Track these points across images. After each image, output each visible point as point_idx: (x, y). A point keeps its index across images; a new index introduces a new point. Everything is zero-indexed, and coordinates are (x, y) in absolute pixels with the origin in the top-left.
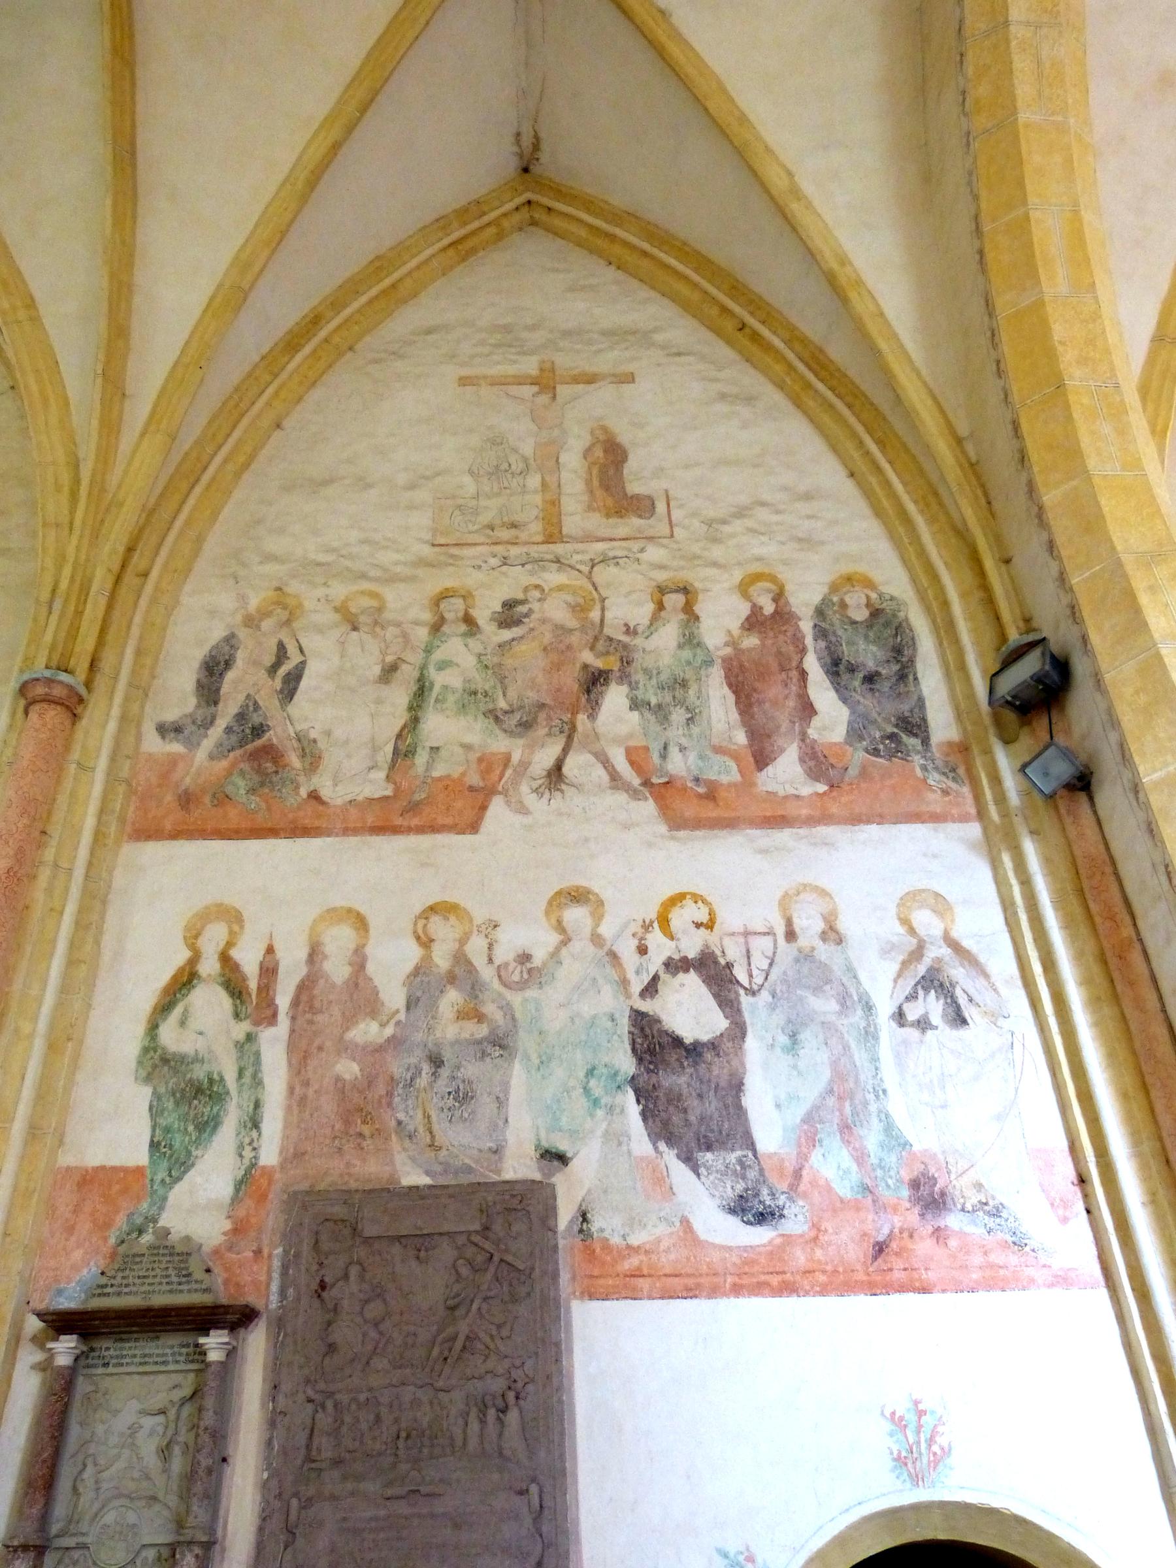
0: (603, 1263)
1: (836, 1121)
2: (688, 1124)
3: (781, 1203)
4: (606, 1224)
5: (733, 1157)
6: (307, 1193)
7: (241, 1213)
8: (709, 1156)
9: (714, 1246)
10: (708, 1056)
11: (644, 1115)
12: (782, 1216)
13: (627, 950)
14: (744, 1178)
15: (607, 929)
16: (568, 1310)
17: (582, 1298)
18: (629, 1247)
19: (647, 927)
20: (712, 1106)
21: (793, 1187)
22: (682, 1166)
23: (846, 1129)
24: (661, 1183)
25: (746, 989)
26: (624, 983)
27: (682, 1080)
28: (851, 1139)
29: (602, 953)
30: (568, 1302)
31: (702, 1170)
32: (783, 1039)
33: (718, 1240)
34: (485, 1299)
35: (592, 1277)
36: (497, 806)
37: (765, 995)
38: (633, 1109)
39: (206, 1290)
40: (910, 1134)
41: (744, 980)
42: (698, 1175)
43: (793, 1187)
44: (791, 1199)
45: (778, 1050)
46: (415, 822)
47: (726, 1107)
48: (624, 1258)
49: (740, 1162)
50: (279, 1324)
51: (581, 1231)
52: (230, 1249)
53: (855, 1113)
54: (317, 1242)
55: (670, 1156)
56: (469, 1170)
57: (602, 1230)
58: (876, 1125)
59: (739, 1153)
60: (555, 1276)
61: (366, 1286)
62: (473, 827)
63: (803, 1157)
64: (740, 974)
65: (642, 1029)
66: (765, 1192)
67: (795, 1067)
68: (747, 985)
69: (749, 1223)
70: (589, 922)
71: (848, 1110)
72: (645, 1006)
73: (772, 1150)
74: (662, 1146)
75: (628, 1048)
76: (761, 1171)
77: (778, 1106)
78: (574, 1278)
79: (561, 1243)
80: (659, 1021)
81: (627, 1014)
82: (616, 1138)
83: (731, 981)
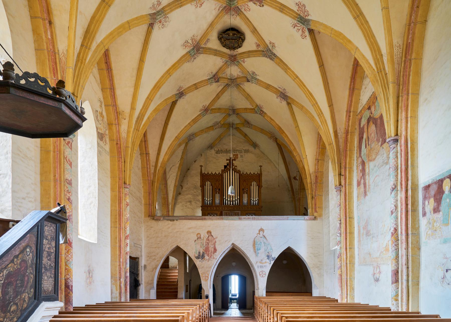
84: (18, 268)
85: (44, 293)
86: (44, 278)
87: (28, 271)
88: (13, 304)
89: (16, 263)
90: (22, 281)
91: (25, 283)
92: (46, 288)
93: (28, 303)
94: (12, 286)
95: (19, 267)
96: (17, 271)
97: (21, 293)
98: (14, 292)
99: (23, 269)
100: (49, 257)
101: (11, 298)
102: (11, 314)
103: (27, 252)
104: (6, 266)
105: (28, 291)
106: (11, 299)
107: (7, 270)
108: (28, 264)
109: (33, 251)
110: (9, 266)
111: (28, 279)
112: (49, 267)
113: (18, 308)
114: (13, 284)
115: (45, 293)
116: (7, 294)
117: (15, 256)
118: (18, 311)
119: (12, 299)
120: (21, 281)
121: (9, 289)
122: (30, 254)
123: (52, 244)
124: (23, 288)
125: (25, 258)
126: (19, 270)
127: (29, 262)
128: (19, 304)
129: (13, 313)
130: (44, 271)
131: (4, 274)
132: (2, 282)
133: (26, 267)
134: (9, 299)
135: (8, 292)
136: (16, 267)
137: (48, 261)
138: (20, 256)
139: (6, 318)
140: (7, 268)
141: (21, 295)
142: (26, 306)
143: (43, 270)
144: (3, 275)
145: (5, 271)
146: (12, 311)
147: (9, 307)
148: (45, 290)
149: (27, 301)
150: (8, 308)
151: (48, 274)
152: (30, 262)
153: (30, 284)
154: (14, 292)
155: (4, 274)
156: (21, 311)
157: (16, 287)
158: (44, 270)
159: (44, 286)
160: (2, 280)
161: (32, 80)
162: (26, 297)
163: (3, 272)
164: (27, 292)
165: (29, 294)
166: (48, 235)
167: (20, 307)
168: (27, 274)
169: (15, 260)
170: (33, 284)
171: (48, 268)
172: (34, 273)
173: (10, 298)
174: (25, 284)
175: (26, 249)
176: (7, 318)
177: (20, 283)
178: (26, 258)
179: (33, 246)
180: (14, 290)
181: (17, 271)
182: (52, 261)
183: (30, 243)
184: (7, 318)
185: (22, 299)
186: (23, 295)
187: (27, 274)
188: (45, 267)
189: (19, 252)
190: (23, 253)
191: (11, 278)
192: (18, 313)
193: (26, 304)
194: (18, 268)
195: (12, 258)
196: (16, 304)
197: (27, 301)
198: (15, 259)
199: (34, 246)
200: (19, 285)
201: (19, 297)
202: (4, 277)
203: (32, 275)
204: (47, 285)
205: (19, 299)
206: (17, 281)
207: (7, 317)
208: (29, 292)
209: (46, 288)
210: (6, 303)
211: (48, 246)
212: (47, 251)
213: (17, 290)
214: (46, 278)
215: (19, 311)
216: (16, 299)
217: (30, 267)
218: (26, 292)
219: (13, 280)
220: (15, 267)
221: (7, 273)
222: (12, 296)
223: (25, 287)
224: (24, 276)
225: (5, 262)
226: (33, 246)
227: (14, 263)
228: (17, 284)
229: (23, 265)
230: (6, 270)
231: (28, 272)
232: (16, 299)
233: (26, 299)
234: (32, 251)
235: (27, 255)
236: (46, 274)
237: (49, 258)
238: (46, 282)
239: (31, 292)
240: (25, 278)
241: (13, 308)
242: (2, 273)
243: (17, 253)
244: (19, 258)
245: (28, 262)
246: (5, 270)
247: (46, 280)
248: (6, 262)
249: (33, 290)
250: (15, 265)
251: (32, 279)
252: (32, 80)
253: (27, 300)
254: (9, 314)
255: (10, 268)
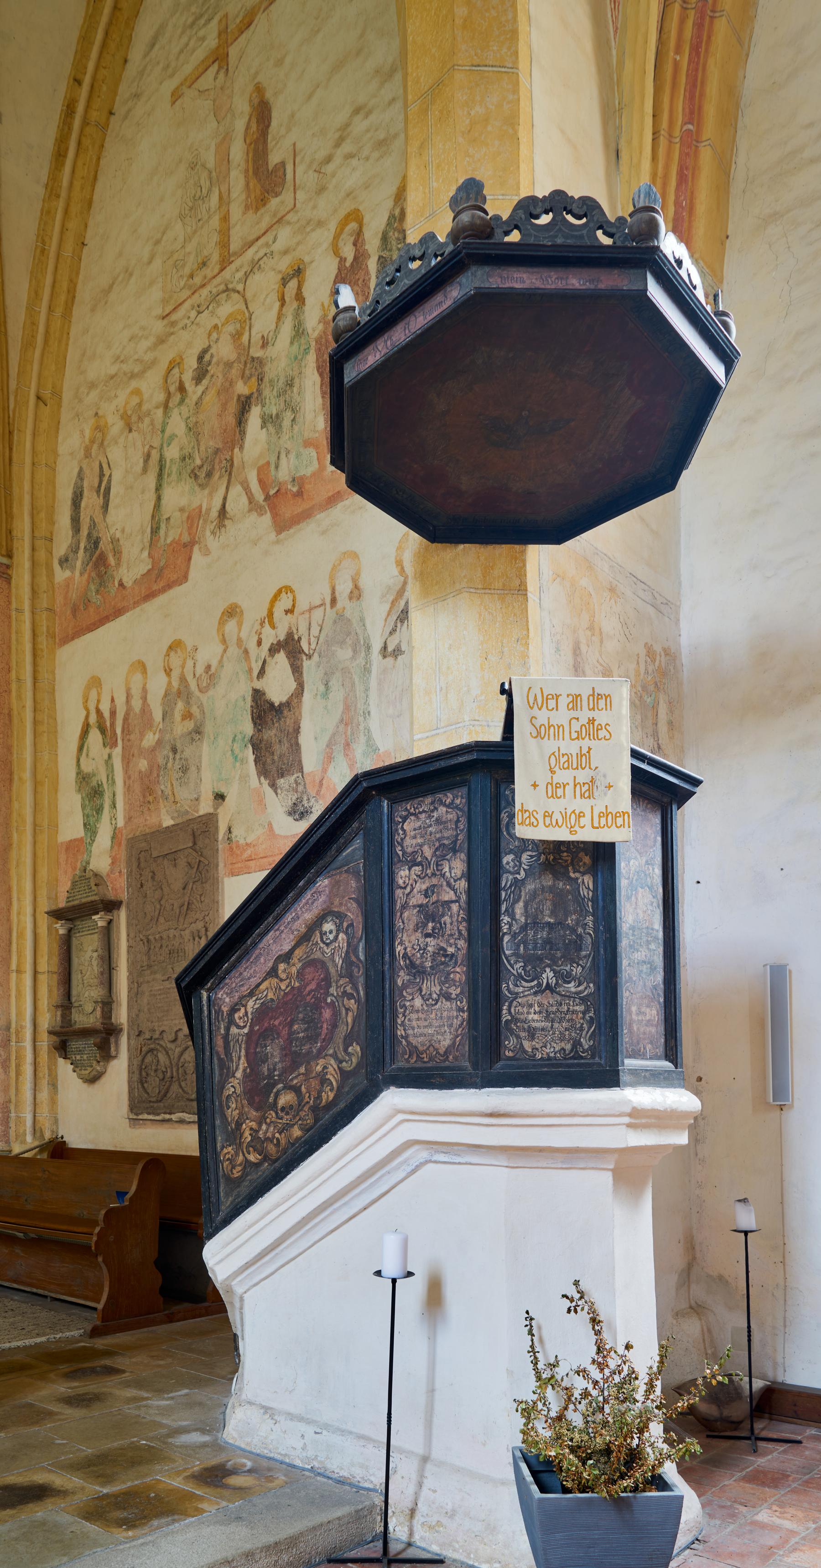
0: (237, 855)
1: (343, 741)
2: (273, 761)
3: (311, 804)
4: (238, 833)
5: (292, 779)
6: (132, 838)
7: (114, 854)
8: (282, 780)
9: (281, 836)
10: (285, 712)
11: (256, 761)
12: (311, 812)
13: (252, 645)
14: (297, 792)
15: (243, 635)
16: (223, 883)
17: (228, 876)
18: (247, 844)
19: (262, 624)
20: (286, 746)
21: (318, 793)
22: (270, 789)
23: (347, 745)
24: (261, 802)
25: (306, 655)
26: (250, 670)
27: (272, 733)
28: (349, 753)
29: (241, 651)
30: (223, 879)
31: (279, 791)
32: (322, 688)
33: (283, 834)
34: (194, 882)
35: (232, 864)
36: (196, 555)
37: (316, 657)
38: (251, 758)
39: (96, 895)
40: (379, 744)
41: (306, 651)
42: (277, 794)
43: (318, 793)
44: (317, 801)
45: (319, 697)
46: (162, 584)
47: (291, 745)
48: (245, 850)
49: (296, 782)
50: (128, 907)
51: (228, 839)
52: (111, 872)
53: (353, 734)
54: (139, 864)
55: (265, 783)
56: (187, 812)
57: (236, 836)
58: (362, 739)
59: (295, 775)
60: (217, 866)
61: (155, 883)
62: (185, 578)
63: (325, 770)
64: (304, 645)
65: (257, 703)
66: (305, 798)
67: (326, 707)
68: (307, 652)
69: (296, 820)
70: (236, 630)
71: (349, 733)
72: (258, 685)
73: (311, 770)
74: (262, 778)
75: (250, 717)
76: (305, 784)
77: (316, 738)
78: (225, 866)
79: (220, 847)
80: (264, 694)
81: (250, 692)
82: (244, 778)
83: (300, 653)
84: (293, 988)
85: (410, 1055)
86: (408, 1004)
87: (333, 990)
88: (284, 1088)
89: (283, 976)
90: (312, 1024)
91: (322, 1027)
92: (420, 1039)
93: (338, 1088)
94: (278, 1038)
95: (297, 984)
96: (290, 997)
97: (309, 1058)
98: (286, 1055)
99: (313, 986)
100: (430, 925)
101: (275, 1070)
102: (281, 1114)
103: (322, 934)
104: (252, 990)
105: (335, 1052)
106: (276, 1073)
107: (257, 999)
108: (332, 971)
109: (351, 925)
110: (263, 987)
111: (336, 1014)
112: (433, 960)
113: (302, 1100)
114: (278, 1034)
115: (418, 1056)
116: (264, 1062)
117: (280, 956)
118: (301, 1110)
119: (279, 1076)
120: (308, 1023)
121: (266, 1046)
122: (336, 938)
123: (447, 869)
124: (317, 1043)
125: (318, 955)
126: (295, 992)
127: (334, 961)
128: (303, 1089)
129: (287, 1114)
130: (409, 981)
131: (250, 1010)
132: (246, 1030)
133: (323, 980)
134: (269, 1075)
135: (267, 1054)
136: (287, 987)
137: (428, 940)
138: (297, 952)
139: (266, 1123)
140: (257, 992)
141: (308, 1063)
142: (331, 1098)
143: (402, 978)
144: (246, 1013)
145: (251, 1003)
146: (283, 1109)
147: (272, 1095)
148: (416, 1047)
149: (334, 1083)
150: (269, 1096)
151: (432, 987)
152: (339, 961)
153: (342, 1031)
154: (286, 1055)
155: (250, 1010)
156: (313, 1111)
157: (290, 1040)
158: (407, 978)
159: (410, 1032)
160: (245, 1027)
161: (545, 219)
162: (330, 1069)
163: (245, 1006)
164: (335, 1056)
165: (341, 1062)
166: (421, 846)
167: (309, 1097)
168: (329, 1000)
169: (282, 966)
170: (356, 1029)
171: (428, 964)
172: (358, 993)
173: (271, 1071)
174: (325, 1031)
175: (321, 925)
176: (269, 1125)
177: (306, 1030)
178: (323, 953)
179: (348, 910)
180: (282, 1049)
181: (290, 997)
182: (451, 935)
183: (337, 901)
184: (269, 1125)
185: (314, 1075)
186: (318, 1064)
187: (329, 1000)
188: (412, 965)
189: (293, 944)
190: (309, 940)
191: (271, 1019)
192: (302, 1114)
193: (331, 1090)
194: (293, 988)
195: (270, 964)
196: (297, 1090)
197: (334, 1083)
198: (282, 965)
199: (355, 905)
200: (301, 1035)
201: (302, 1070)
202: (250, 1016)
203: (353, 1001)
204: (426, 1027)
205: (303, 1074)
206: (291, 1024)
207: (268, 1120)
208: (341, 1054)
209: (420, 1039)
210: (262, 1084)
211: (422, 886)
212: (420, 906)
213: (293, 1049)
214: (418, 1002)
215: (306, 1109)
216: (294, 1075)
217: (341, 976)
218: (331, 1055)
219: (276, 1023)
220: (283, 987)
221: (256, 1006)
222: (280, 1066)
223: (324, 1040)
224: (317, 1007)
225: (249, 978)
226: (348, 910)
227: (277, 976)
228: (291, 1033)
229: (309, 977)
230: (254, 998)
231: (332, 995)
232: (294, 1075)
233: (328, 1076)
234: (345, 924)
235: (324, 943)
236: (421, 990)
237: (434, 928)
238: (418, 1019)
239: (349, 1054)
240: (321, 1013)
241: (286, 1099)
242: (243, 1010)
243: (287, 948)
244: (295, 960)
245: (330, 965)
246: (251, 1001)
247: (418, 1011)
248: (252, 980)
249: (358, 1049)
250: (281, 980)
251: (350, 1014)
252: (545, 219)
253: (333, 1077)
254: (274, 1115)
255: (265, 993)
